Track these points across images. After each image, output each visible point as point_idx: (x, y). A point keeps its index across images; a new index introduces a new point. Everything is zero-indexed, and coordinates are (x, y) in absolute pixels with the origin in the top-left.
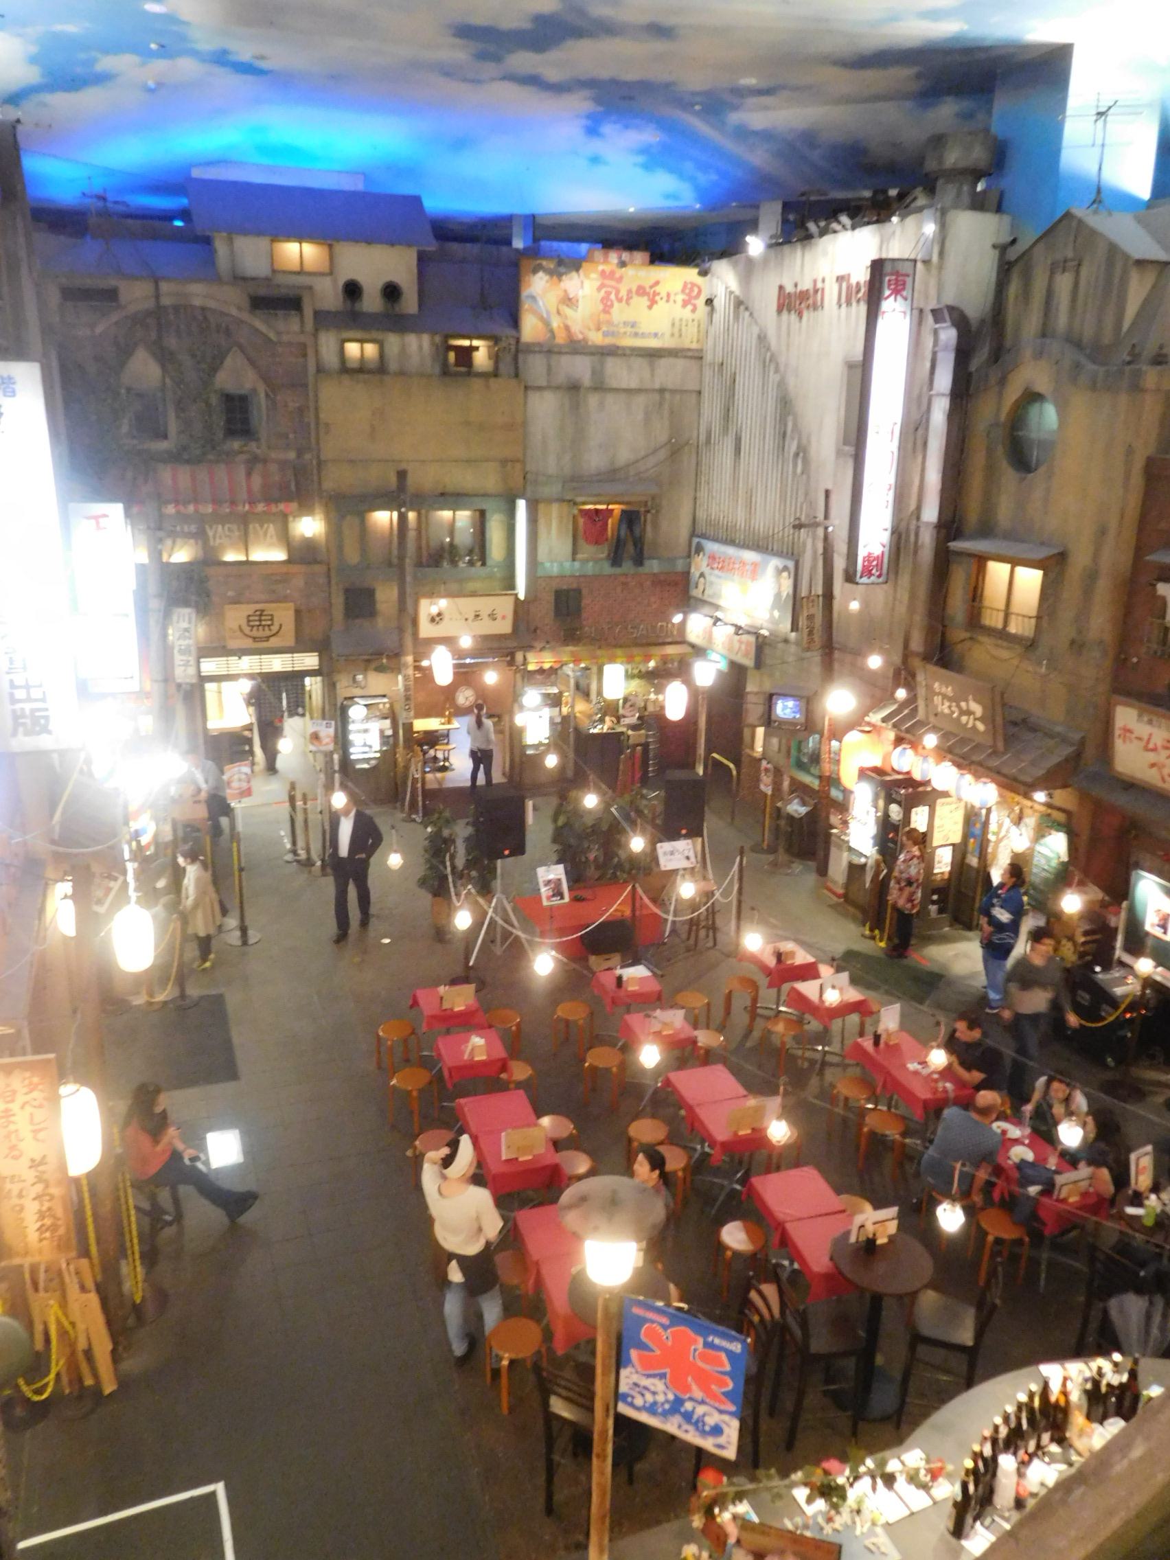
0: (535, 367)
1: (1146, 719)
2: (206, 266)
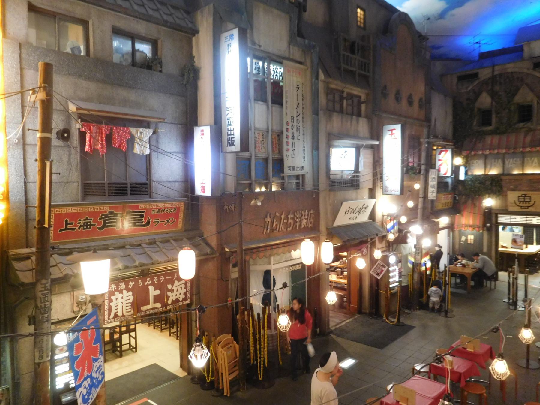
2: (521, 58)
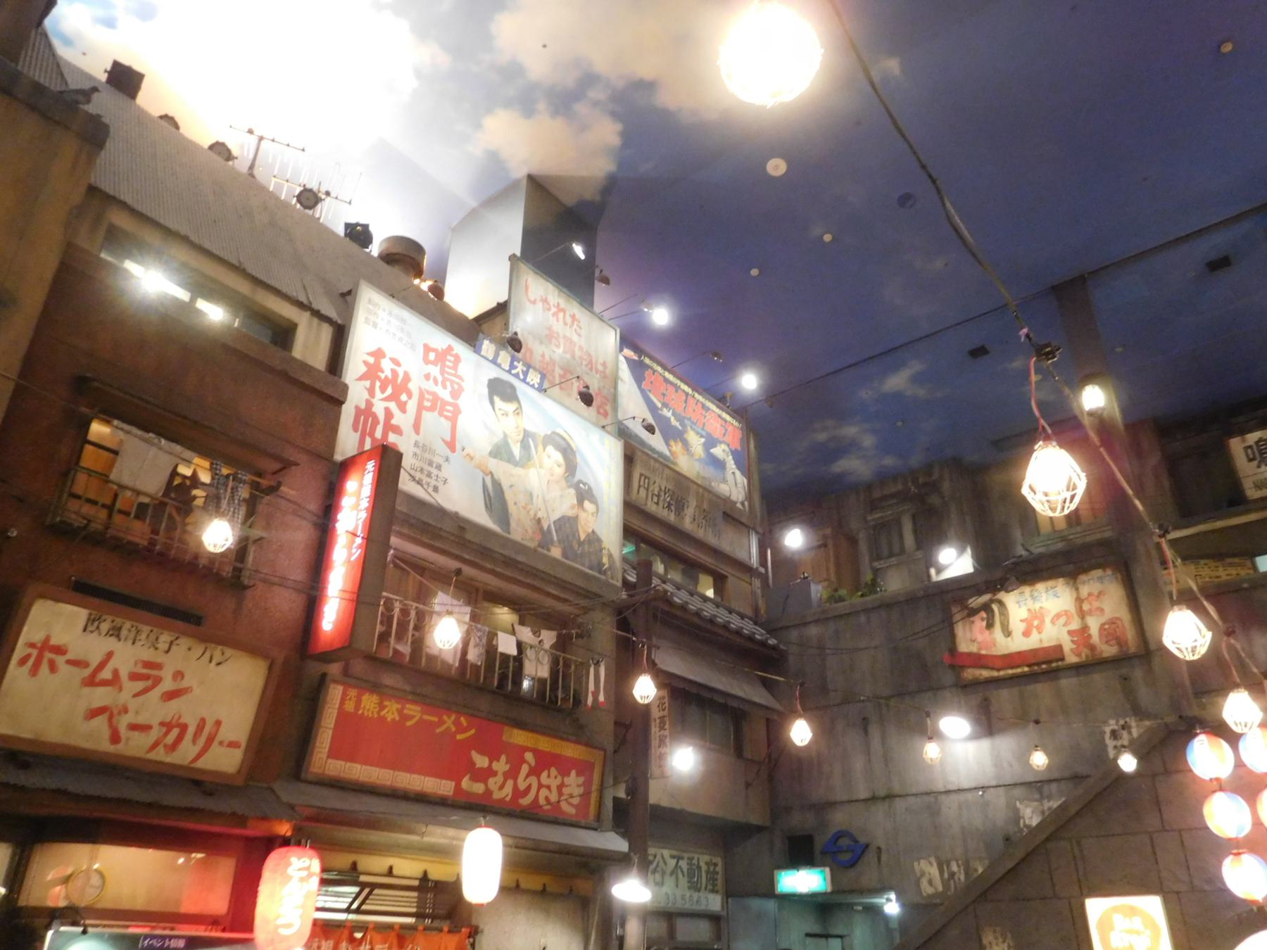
1: (105, 627)
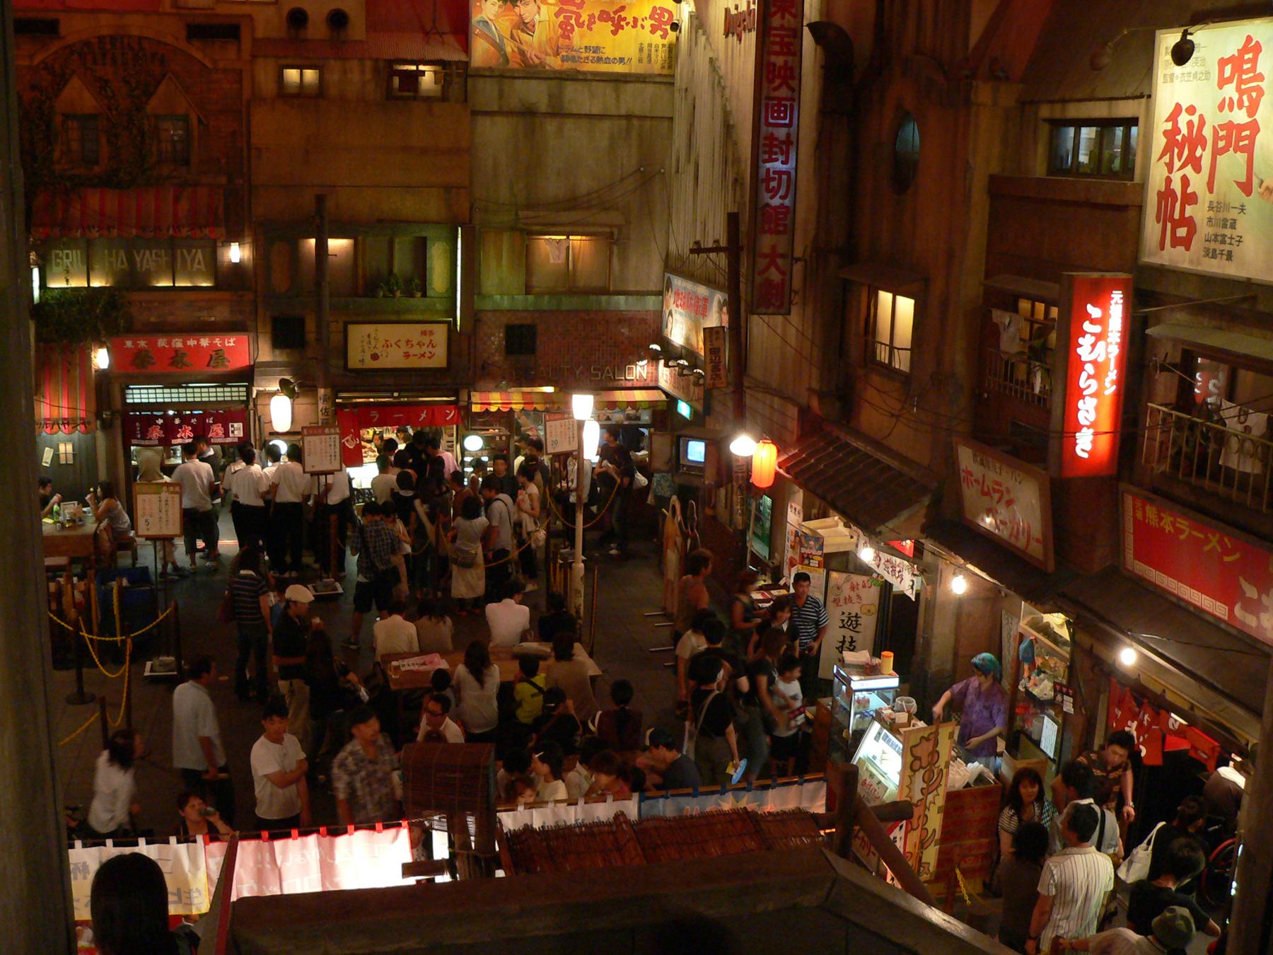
0: (486, 93)
